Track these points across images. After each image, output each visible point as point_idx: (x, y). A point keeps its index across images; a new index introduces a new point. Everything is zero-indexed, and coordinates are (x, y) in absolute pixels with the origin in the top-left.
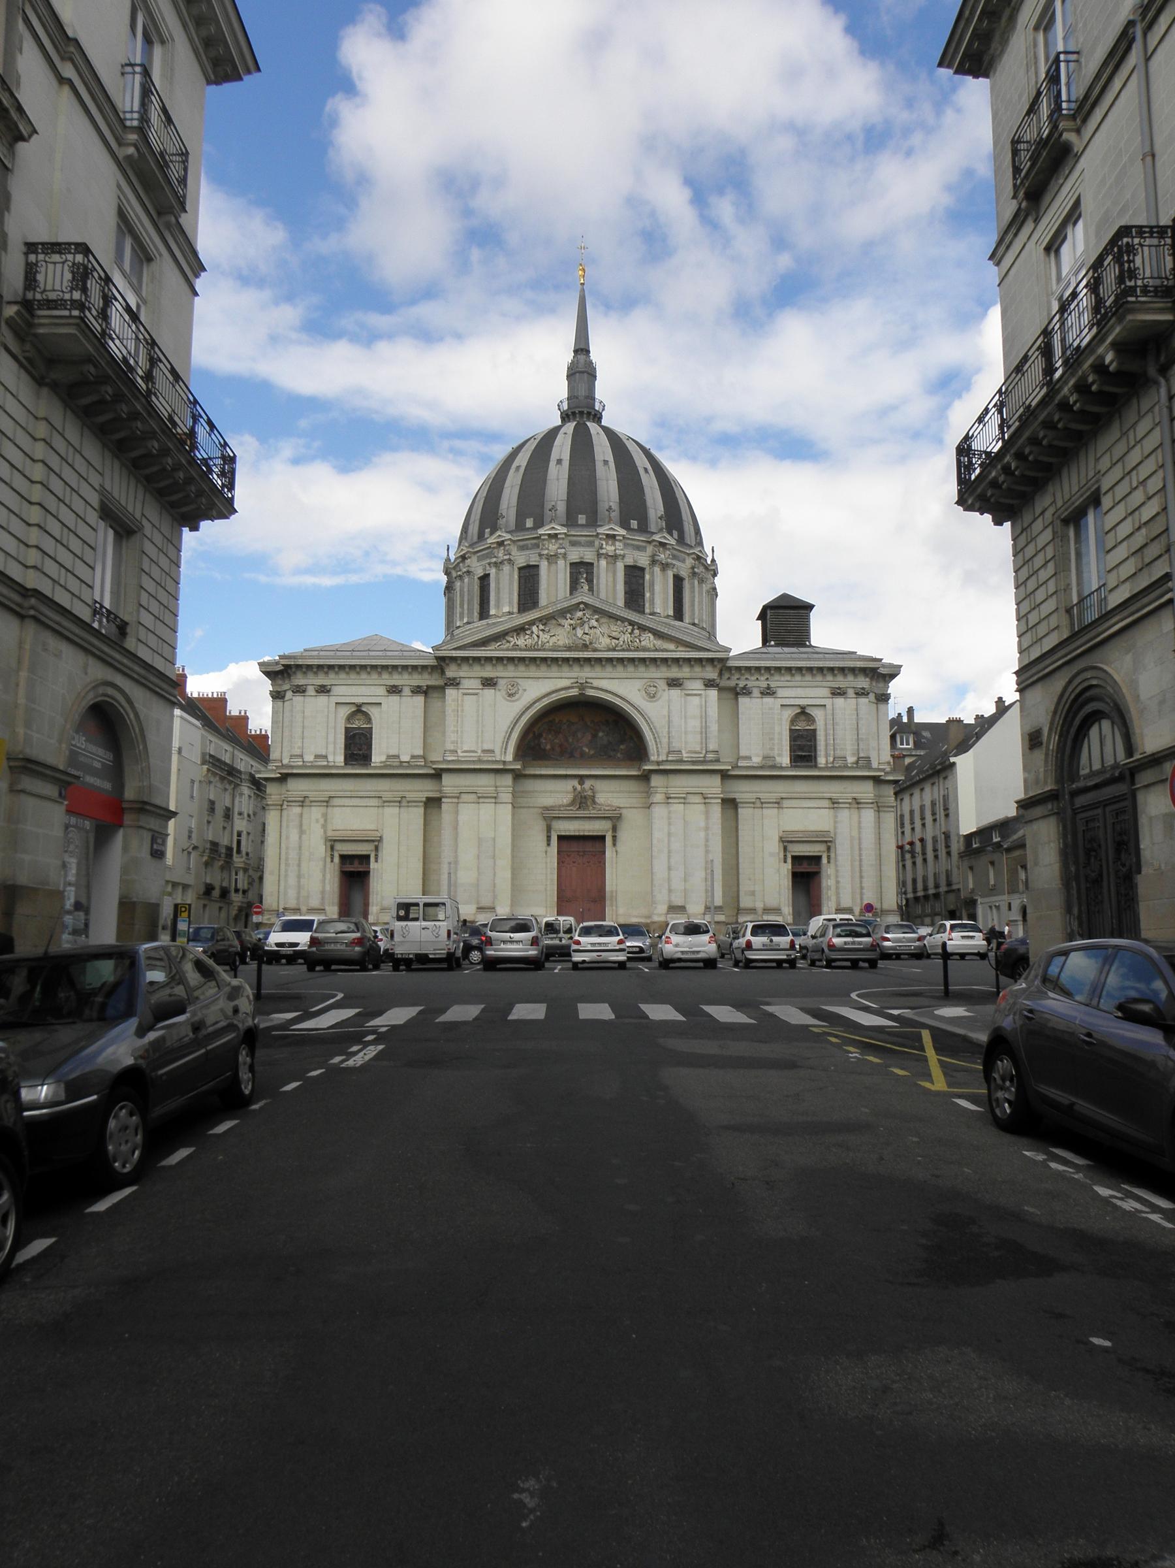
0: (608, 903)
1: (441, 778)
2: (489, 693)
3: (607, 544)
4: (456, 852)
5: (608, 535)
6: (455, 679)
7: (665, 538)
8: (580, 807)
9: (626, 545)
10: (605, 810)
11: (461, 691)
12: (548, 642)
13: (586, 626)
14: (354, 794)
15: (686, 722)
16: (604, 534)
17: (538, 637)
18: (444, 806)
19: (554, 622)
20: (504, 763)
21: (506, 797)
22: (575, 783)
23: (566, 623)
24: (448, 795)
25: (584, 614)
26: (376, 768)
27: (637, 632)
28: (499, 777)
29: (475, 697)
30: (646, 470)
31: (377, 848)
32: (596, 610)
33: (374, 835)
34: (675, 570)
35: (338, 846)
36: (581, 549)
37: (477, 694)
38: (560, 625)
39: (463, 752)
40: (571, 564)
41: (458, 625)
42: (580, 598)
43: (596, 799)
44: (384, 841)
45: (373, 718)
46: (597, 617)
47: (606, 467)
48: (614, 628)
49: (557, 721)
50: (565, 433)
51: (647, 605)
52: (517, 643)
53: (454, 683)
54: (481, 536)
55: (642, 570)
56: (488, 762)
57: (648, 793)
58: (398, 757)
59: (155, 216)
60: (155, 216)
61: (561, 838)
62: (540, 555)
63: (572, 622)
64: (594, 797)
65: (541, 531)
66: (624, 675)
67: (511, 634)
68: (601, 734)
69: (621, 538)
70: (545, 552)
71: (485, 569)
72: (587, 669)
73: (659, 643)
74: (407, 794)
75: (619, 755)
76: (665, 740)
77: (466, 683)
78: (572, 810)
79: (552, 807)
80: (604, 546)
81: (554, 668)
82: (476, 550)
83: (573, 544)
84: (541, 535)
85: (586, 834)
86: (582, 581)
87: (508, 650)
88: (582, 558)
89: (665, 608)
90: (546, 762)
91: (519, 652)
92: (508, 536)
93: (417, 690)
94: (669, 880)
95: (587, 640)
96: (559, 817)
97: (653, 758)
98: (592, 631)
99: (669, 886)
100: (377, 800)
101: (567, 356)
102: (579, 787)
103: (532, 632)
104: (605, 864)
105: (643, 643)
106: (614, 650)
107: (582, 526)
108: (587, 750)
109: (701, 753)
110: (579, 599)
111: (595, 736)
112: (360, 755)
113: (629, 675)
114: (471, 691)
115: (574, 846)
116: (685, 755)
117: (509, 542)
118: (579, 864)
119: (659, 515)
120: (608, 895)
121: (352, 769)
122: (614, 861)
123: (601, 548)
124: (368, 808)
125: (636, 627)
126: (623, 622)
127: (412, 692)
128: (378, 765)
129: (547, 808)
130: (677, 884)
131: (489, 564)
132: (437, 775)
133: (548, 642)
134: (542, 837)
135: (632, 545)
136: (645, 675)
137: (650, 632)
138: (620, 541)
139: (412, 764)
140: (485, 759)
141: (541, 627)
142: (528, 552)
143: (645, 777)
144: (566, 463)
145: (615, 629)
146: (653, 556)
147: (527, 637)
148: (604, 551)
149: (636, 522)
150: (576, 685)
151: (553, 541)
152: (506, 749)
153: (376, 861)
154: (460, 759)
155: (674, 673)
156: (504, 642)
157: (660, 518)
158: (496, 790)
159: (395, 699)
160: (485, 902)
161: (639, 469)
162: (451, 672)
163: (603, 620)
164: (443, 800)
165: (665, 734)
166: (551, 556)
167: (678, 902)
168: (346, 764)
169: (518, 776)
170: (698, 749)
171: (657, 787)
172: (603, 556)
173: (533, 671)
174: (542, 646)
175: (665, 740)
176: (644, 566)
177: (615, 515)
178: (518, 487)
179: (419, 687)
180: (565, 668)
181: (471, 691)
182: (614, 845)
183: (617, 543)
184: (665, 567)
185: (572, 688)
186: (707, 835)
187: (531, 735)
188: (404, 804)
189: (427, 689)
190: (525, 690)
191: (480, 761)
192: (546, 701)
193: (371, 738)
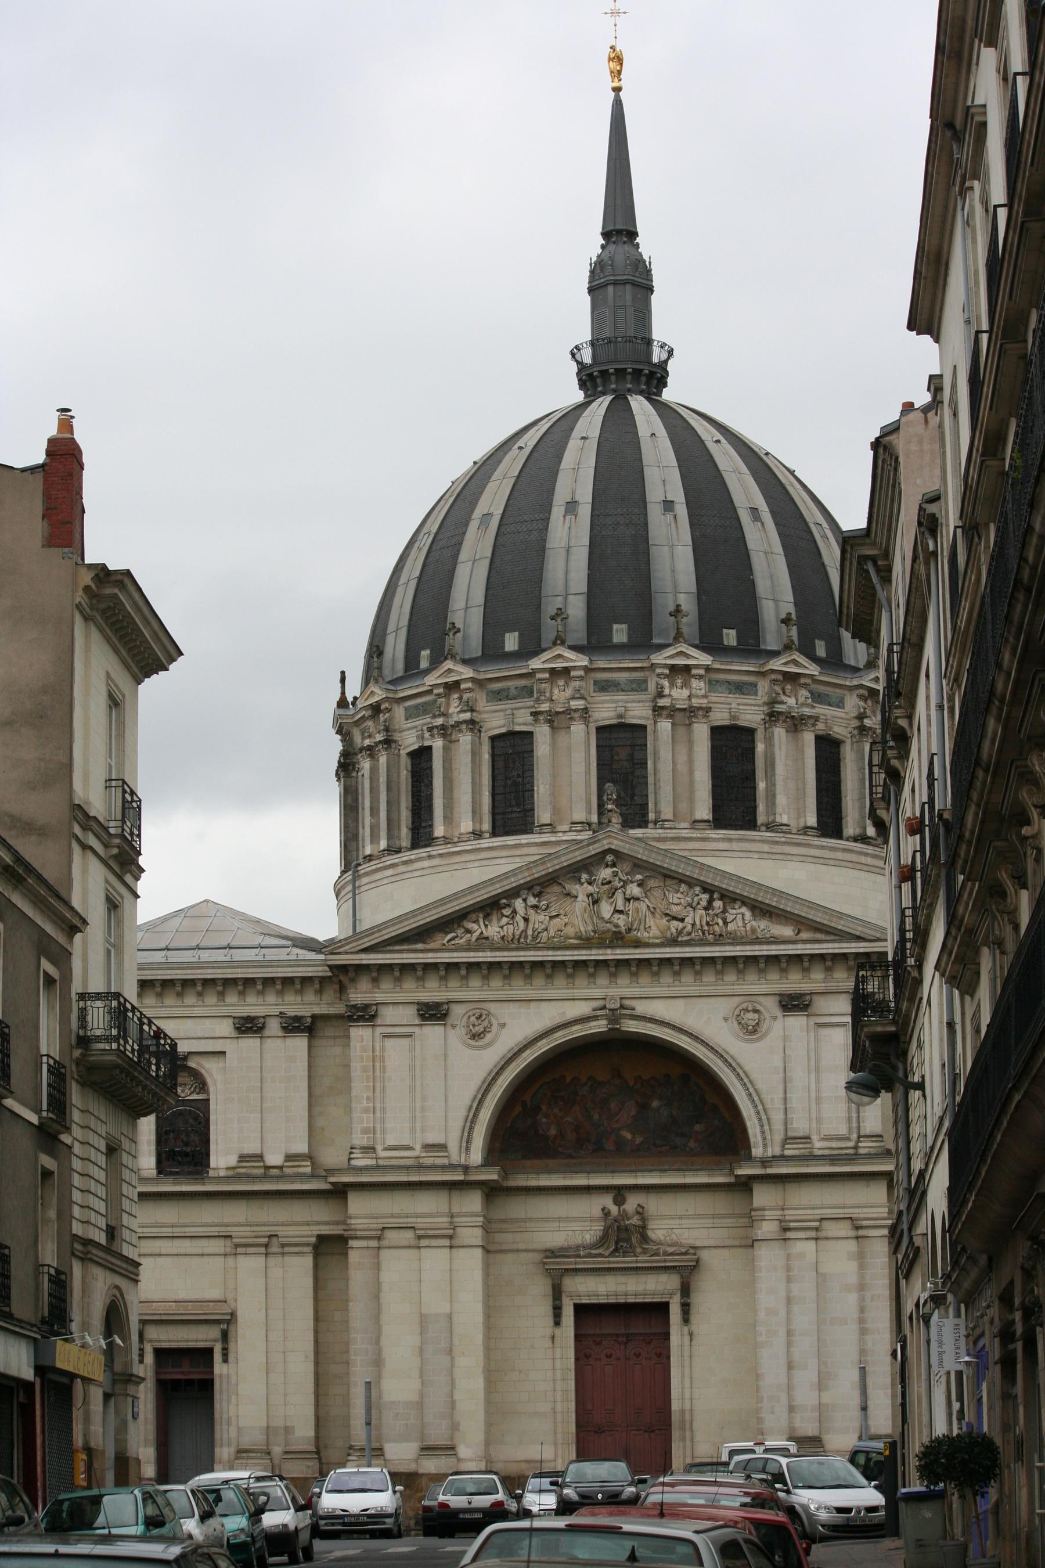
0: (675, 1434)
1: (346, 1198)
2: (433, 1032)
3: (672, 685)
4: (378, 1341)
5: (673, 668)
6: (366, 1007)
7: (795, 662)
8: (616, 1250)
9: (712, 684)
10: (666, 1254)
11: (379, 1030)
12: (546, 929)
13: (619, 897)
14: (179, 1232)
15: (818, 1081)
16: (665, 666)
17: (526, 920)
18: (354, 1256)
19: (556, 888)
20: (466, 1169)
21: (473, 1235)
22: (607, 1201)
23: (582, 891)
24: (359, 1233)
25: (615, 874)
26: (219, 1179)
27: (718, 904)
28: (456, 1195)
29: (405, 1041)
30: (754, 511)
31: (225, 1336)
32: (638, 865)
33: (219, 1312)
34: (820, 726)
35: (152, 1332)
36: (621, 697)
37: (409, 1036)
38: (568, 894)
39: (386, 1149)
40: (600, 730)
41: (368, 851)
42: (605, 842)
43: (650, 1233)
44: (240, 1319)
45: (209, 1081)
46: (639, 877)
47: (669, 517)
48: (673, 897)
49: (568, 1080)
50: (583, 438)
51: (761, 808)
52: (485, 934)
53: (365, 1015)
55: (750, 732)
56: (434, 1167)
57: (751, 1218)
58: (260, 1157)
59: (117, 869)
60: (117, 869)
61: (581, 1310)
62: (535, 714)
63: (590, 889)
64: (644, 1227)
65: (535, 663)
66: (694, 990)
67: (473, 916)
68: (655, 1104)
69: (702, 672)
70: (545, 707)
71: (422, 737)
72: (624, 980)
73: (763, 925)
74: (280, 1231)
75: (692, 1144)
76: (777, 1117)
77: (389, 1015)
79: (562, 1249)
80: (667, 691)
81: (560, 980)
82: (401, 695)
83: (604, 687)
84: (534, 672)
85: (631, 1300)
86: (610, 807)
87: (468, 948)
88: (620, 716)
89: (800, 812)
90: (552, 1163)
91: (489, 954)
92: (467, 672)
93: (293, 1026)
94: (790, 1387)
95: (621, 923)
96: (576, 1270)
97: (757, 1151)
98: (632, 905)
99: (790, 1398)
100: (221, 1242)
101: (593, 245)
102: (614, 1210)
103: (515, 912)
104: (669, 1358)
105: (731, 927)
106: (673, 942)
107: (621, 648)
108: (629, 1136)
109: (848, 1139)
110: (605, 844)
111: (643, 1107)
112: (186, 1154)
113: (704, 990)
114: (398, 1030)
115: (609, 1327)
116: (818, 1144)
117: (469, 685)
118: (618, 1359)
119: (783, 616)
120: (675, 1418)
121: (175, 1184)
122: (686, 1354)
123: (660, 695)
124: (206, 1259)
125: (716, 896)
126: (690, 886)
127: (284, 1028)
128: (222, 1173)
129: (552, 1253)
130: (806, 1396)
131: (430, 729)
132: (339, 1193)
133: (546, 929)
134: (545, 1308)
135: (728, 682)
136: (739, 989)
137: (744, 903)
138: (701, 677)
139: (287, 1171)
140: (429, 1161)
141: (532, 901)
142: (510, 705)
143: (745, 1185)
144: (585, 511)
145: (676, 901)
146: (773, 702)
147: (505, 920)
148: (662, 702)
149: (733, 633)
150: (599, 1013)
151: (561, 682)
152: (468, 1142)
153: (225, 1360)
154: (381, 1162)
155: (794, 983)
156: (460, 931)
157: (786, 621)
158: (451, 1223)
159: (250, 1043)
160: (437, 1436)
162: (360, 994)
163: (652, 883)
164: (352, 1243)
165: (778, 1104)
166: (558, 713)
167: (809, 1429)
168: (159, 1172)
169: (492, 1192)
170: (843, 1130)
171: (764, 1209)
172: (665, 713)
173: (519, 988)
174: (534, 938)
175: (777, 1117)
176: (754, 726)
177: (690, 622)
178: (486, 563)
179: (297, 1019)
180: (581, 980)
181: (398, 1030)
182: (686, 1320)
183: (695, 683)
184: (796, 724)
185: (595, 1018)
186: (862, 1299)
187: (518, 1109)
188: (274, 1249)
189: (313, 1023)
190: (503, 1025)
191: (421, 1167)
192: (544, 1046)
193: (208, 1120)
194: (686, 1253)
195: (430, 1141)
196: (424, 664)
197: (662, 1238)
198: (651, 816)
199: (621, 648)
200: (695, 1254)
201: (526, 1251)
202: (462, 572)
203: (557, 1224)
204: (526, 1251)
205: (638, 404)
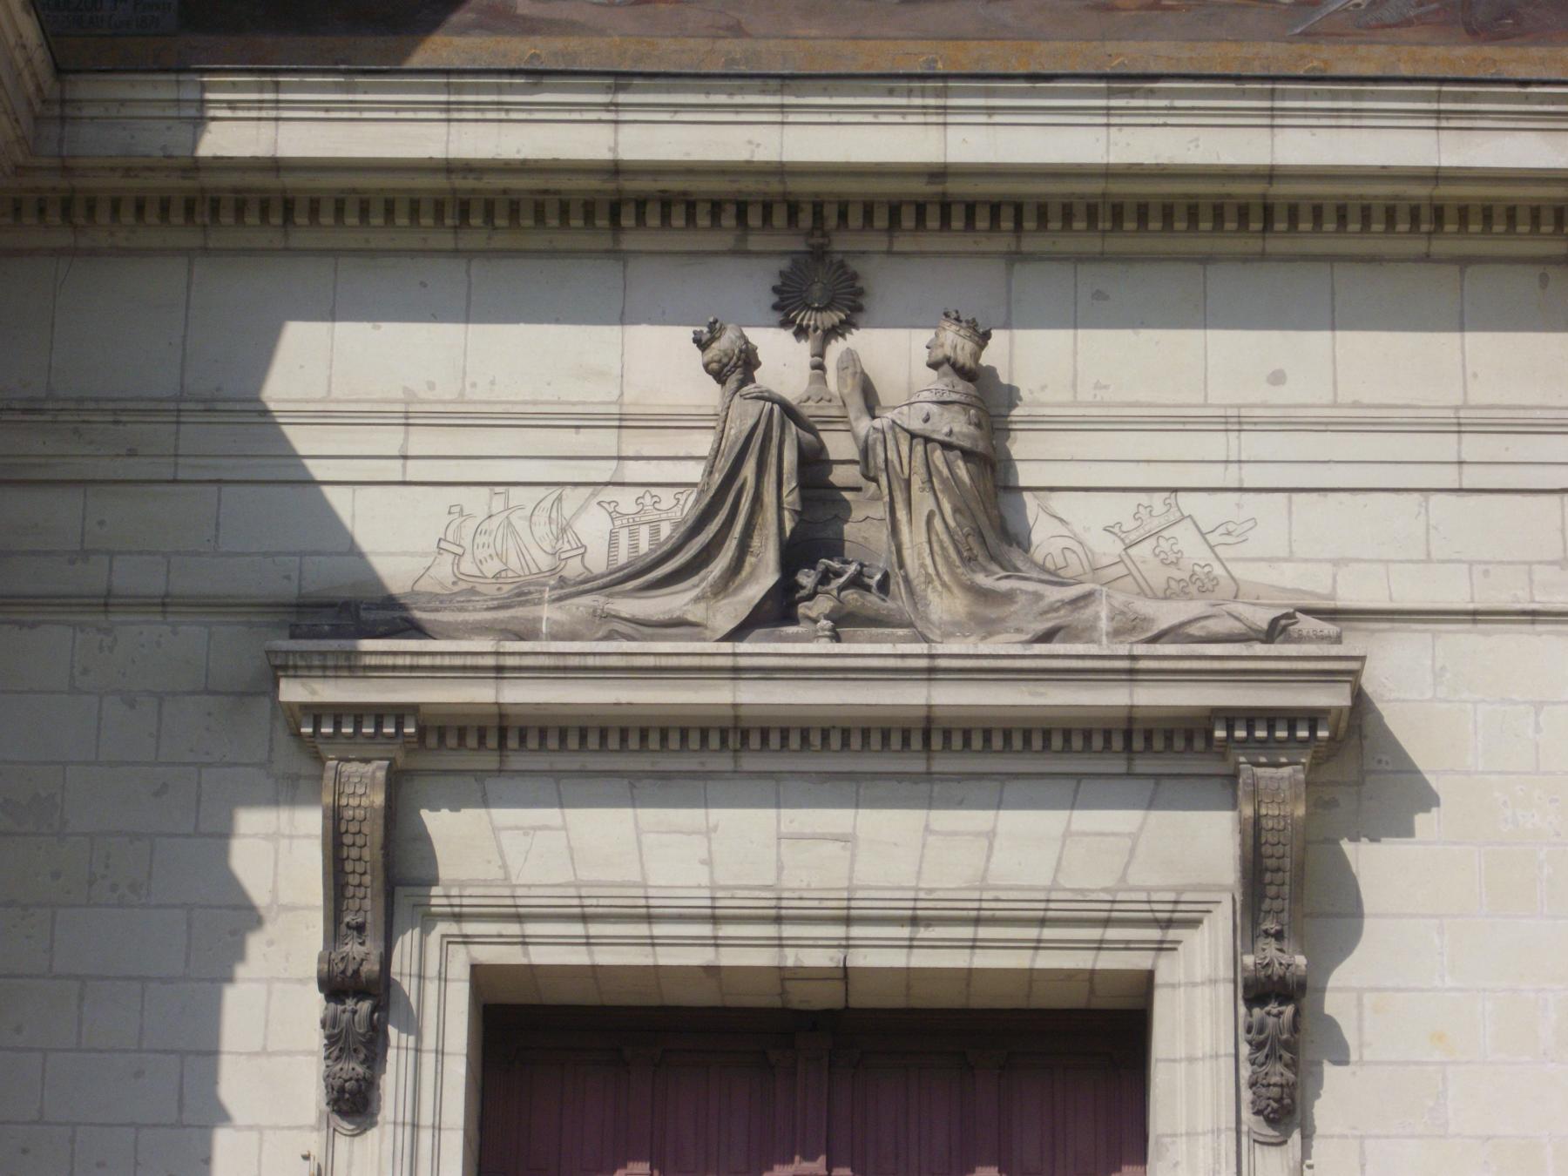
10: (1127, 626)
78: (676, 625)
194: (1276, 631)
197: (1107, 549)
200: (1338, 640)
201: (164, 604)
203: (389, 440)
204: (164, 604)
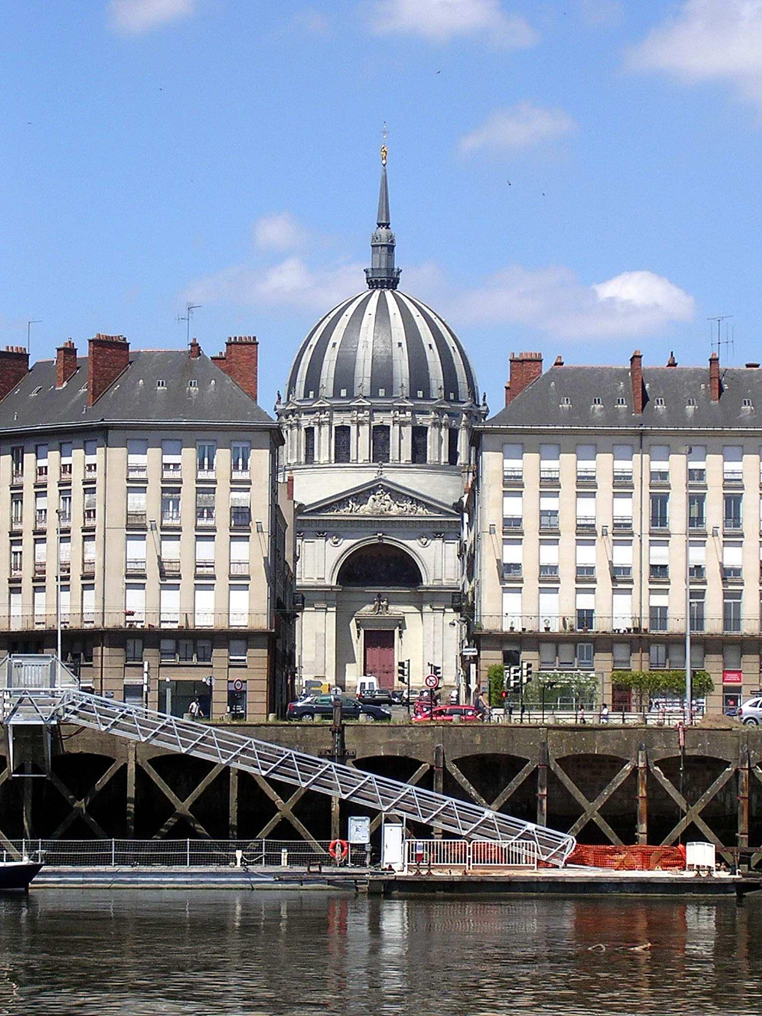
30: (430, 345)
54: (306, 395)
62: (352, 421)
97: (425, 583)
141: (355, 499)
148: (396, 419)
149: (421, 392)
161: (425, 346)
170: (453, 578)
177: (406, 392)
182: (401, 637)
195: (320, 577)
196: (311, 396)
198: (391, 458)
199: (382, 398)
202: (326, 364)
205: (388, 294)
